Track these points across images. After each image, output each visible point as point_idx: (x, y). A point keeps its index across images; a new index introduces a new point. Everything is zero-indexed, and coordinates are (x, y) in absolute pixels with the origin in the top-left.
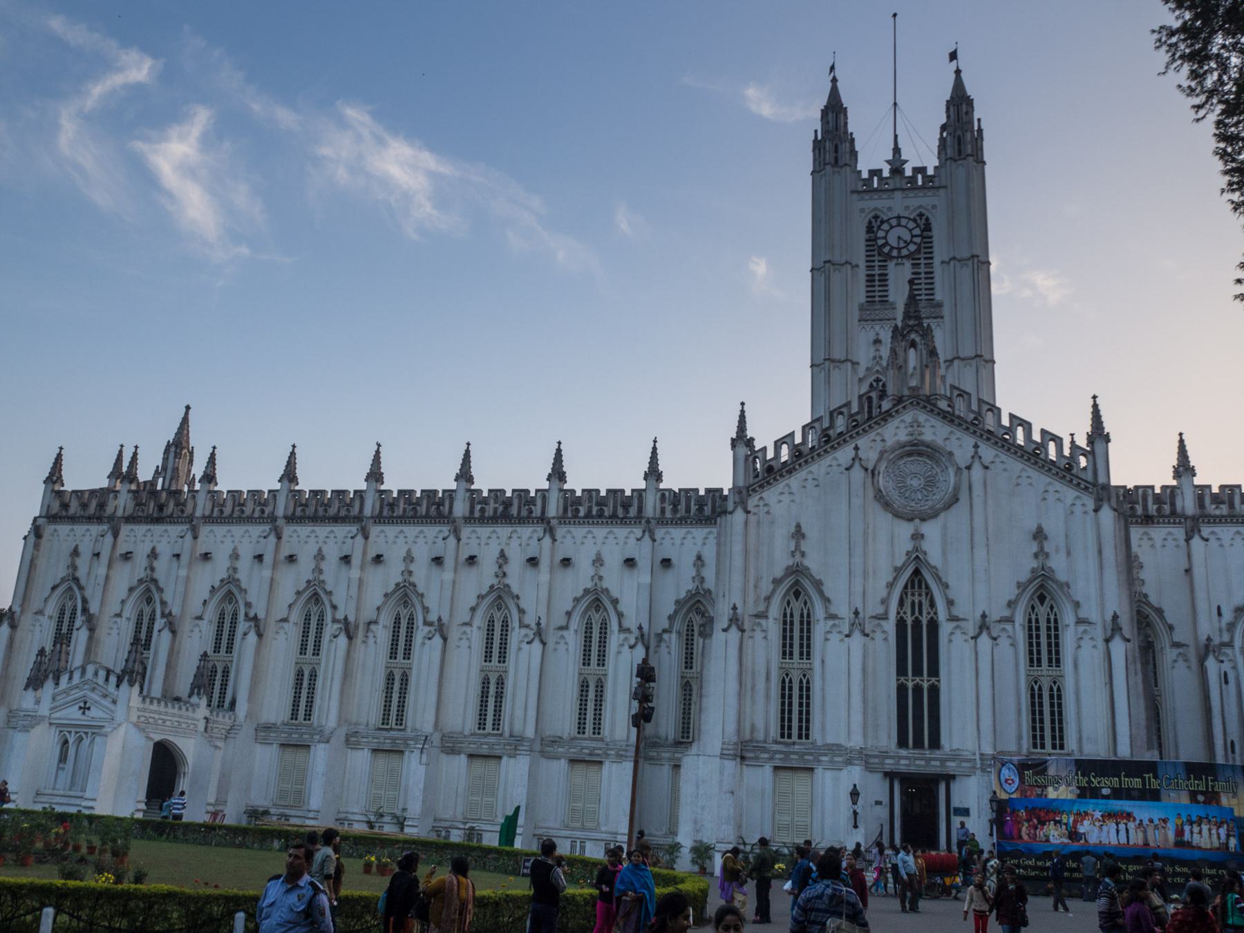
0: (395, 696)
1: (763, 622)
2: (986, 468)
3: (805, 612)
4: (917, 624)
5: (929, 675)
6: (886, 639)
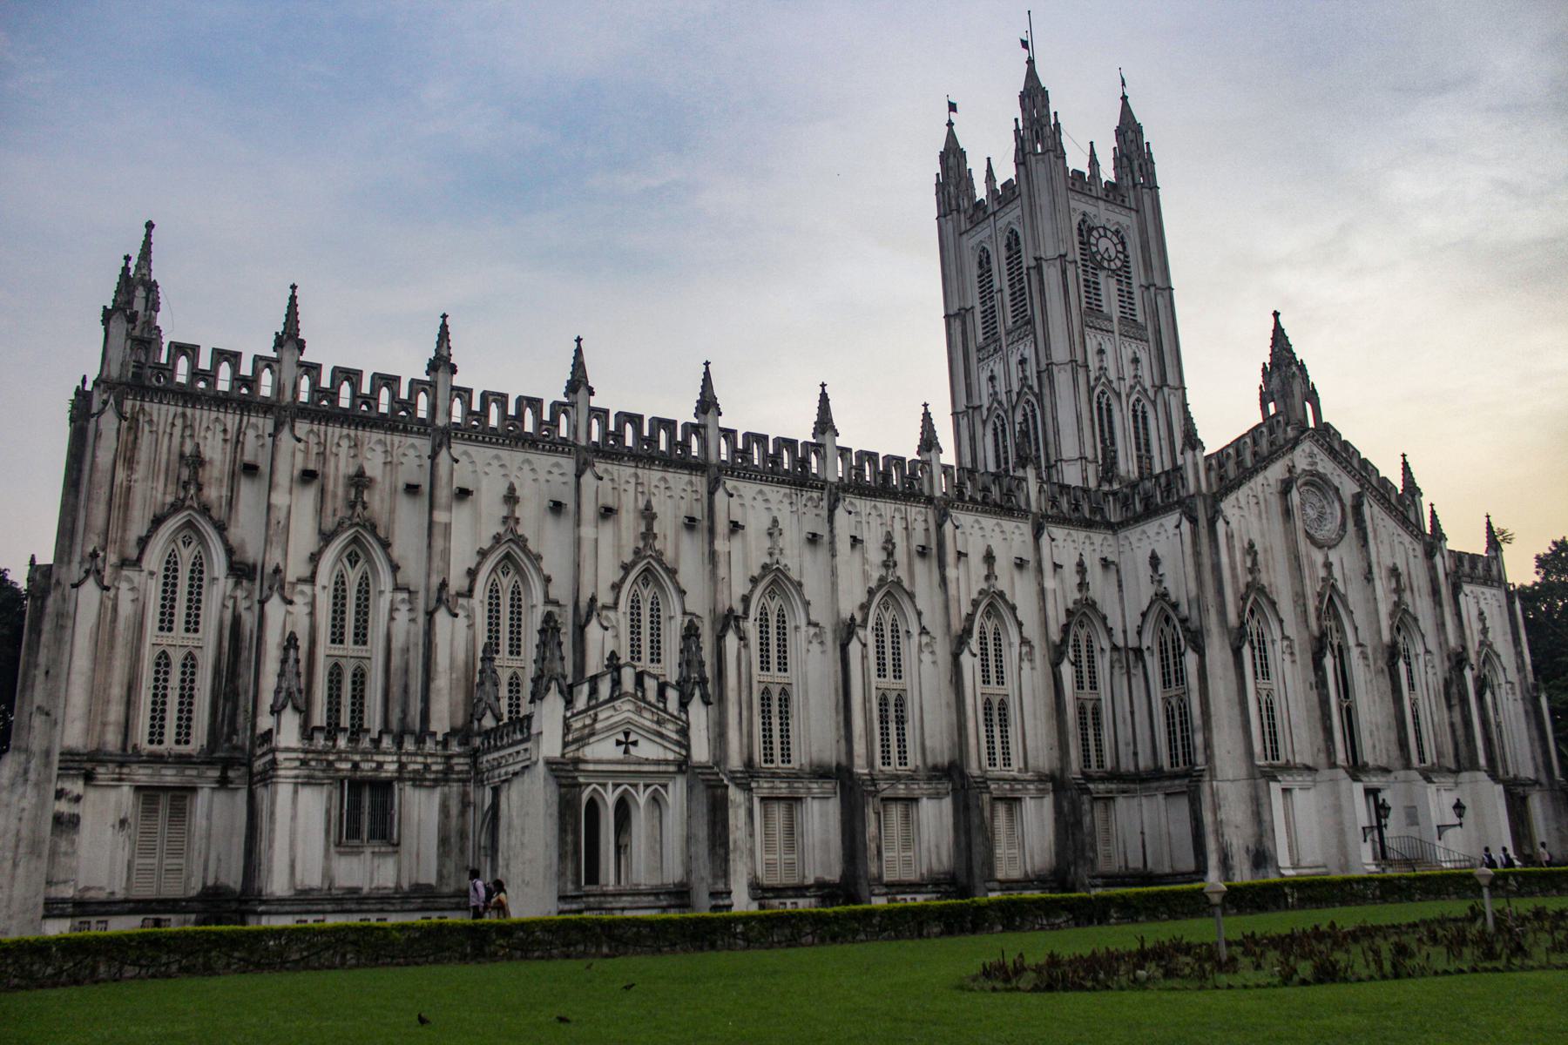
0: (776, 721)
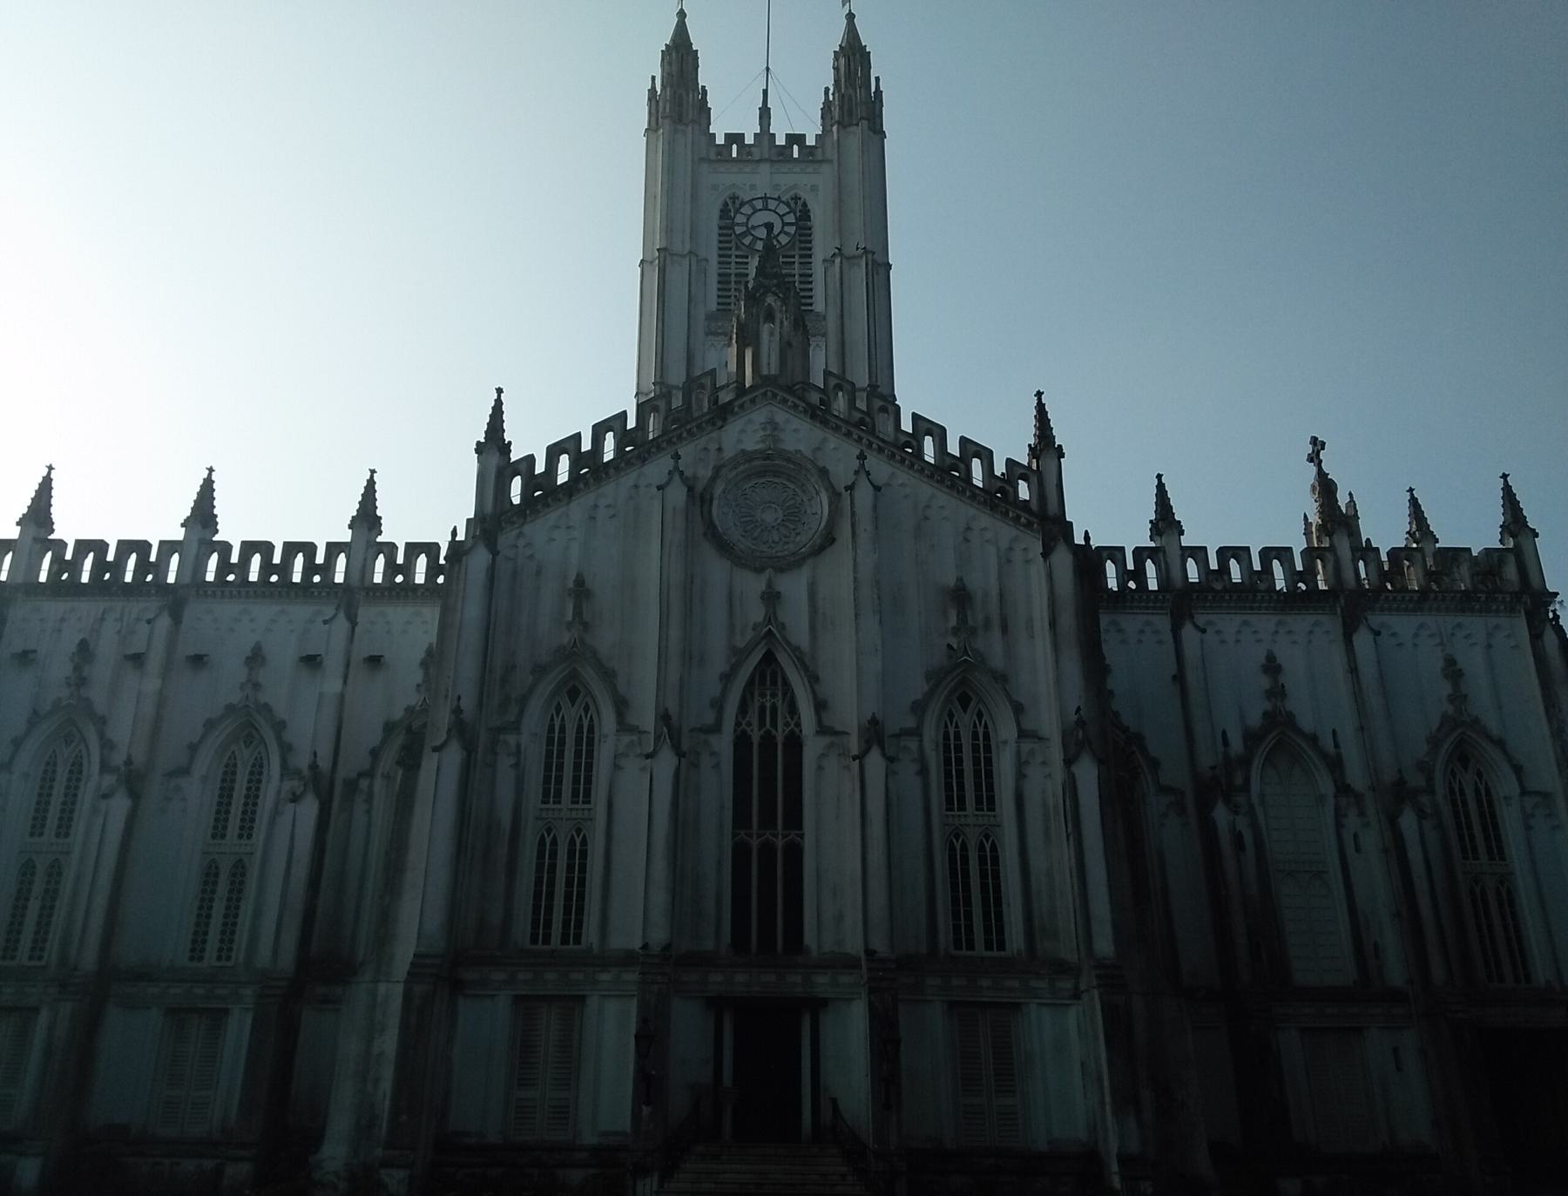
1: (511, 739)
2: (877, 489)
3: (586, 724)
4: (768, 741)
5: (786, 827)
6: (717, 766)
